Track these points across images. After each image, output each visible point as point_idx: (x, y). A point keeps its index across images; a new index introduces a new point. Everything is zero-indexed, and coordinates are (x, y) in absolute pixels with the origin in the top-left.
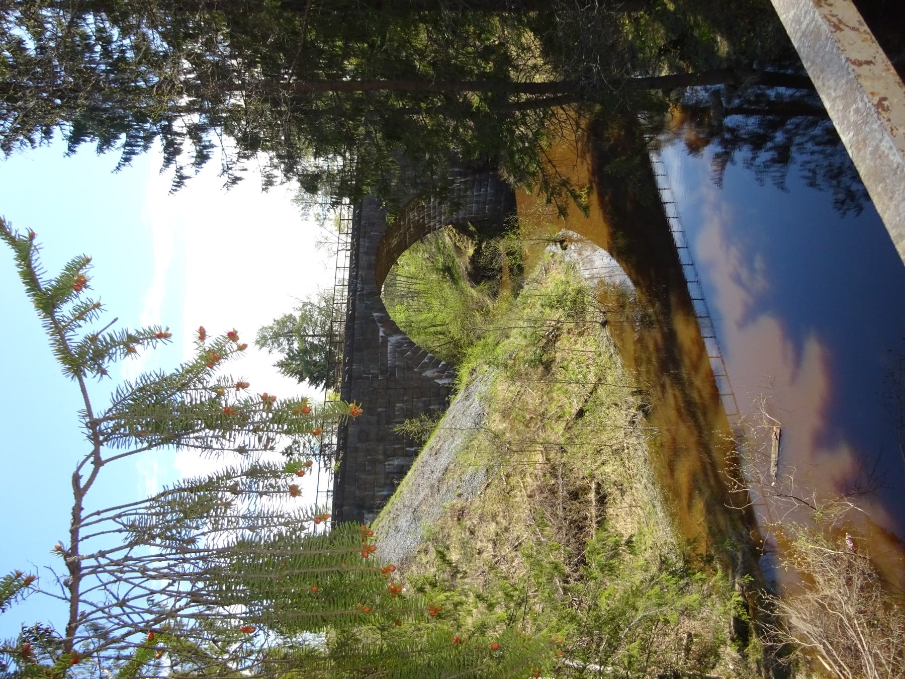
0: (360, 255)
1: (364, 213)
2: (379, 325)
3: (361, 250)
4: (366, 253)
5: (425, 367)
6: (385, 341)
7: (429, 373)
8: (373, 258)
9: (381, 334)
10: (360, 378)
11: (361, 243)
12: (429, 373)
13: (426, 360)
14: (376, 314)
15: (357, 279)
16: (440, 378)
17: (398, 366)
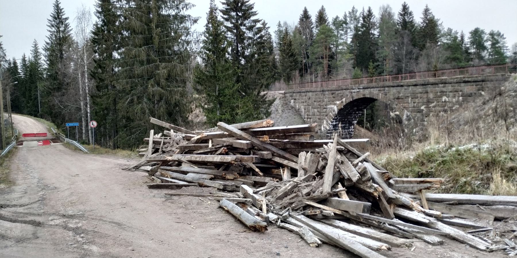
0: (369, 89)
1: (392, 88)
2: (340, 101)
3: (372, 89)
4: (370, 93)
5: (327, 122)
6: (335, 104)
7: (325, 122)
8: (368, 96)
9: (338, 102)
10: (324, 95)
11: (375, 89)
12: (325, 122)
13: (329, 122)
14: (344, 100)
15: (359, 89)
16: (324, 127)
17: (326, 111)
